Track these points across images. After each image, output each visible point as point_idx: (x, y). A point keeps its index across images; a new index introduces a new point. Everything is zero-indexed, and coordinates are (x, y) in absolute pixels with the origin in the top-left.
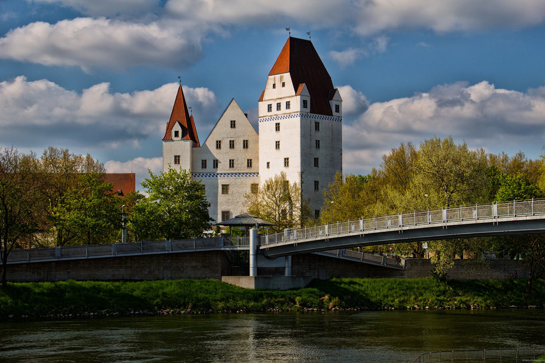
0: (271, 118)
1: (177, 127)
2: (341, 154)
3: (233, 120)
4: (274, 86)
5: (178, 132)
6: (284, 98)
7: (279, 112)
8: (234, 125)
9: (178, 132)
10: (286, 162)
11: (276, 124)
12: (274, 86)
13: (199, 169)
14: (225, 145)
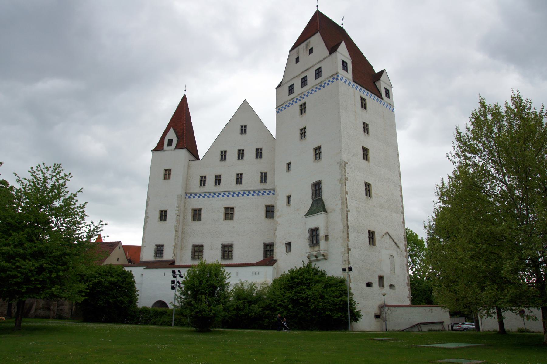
1: (172, 135)
2: (398, 155)
3: (243, 124)
5: (172, 140)
6: (311, 67)
8: (245, 130)
9: (172, 140)
10: (318, 151)
13: (195, 187)
14: (232, 156)
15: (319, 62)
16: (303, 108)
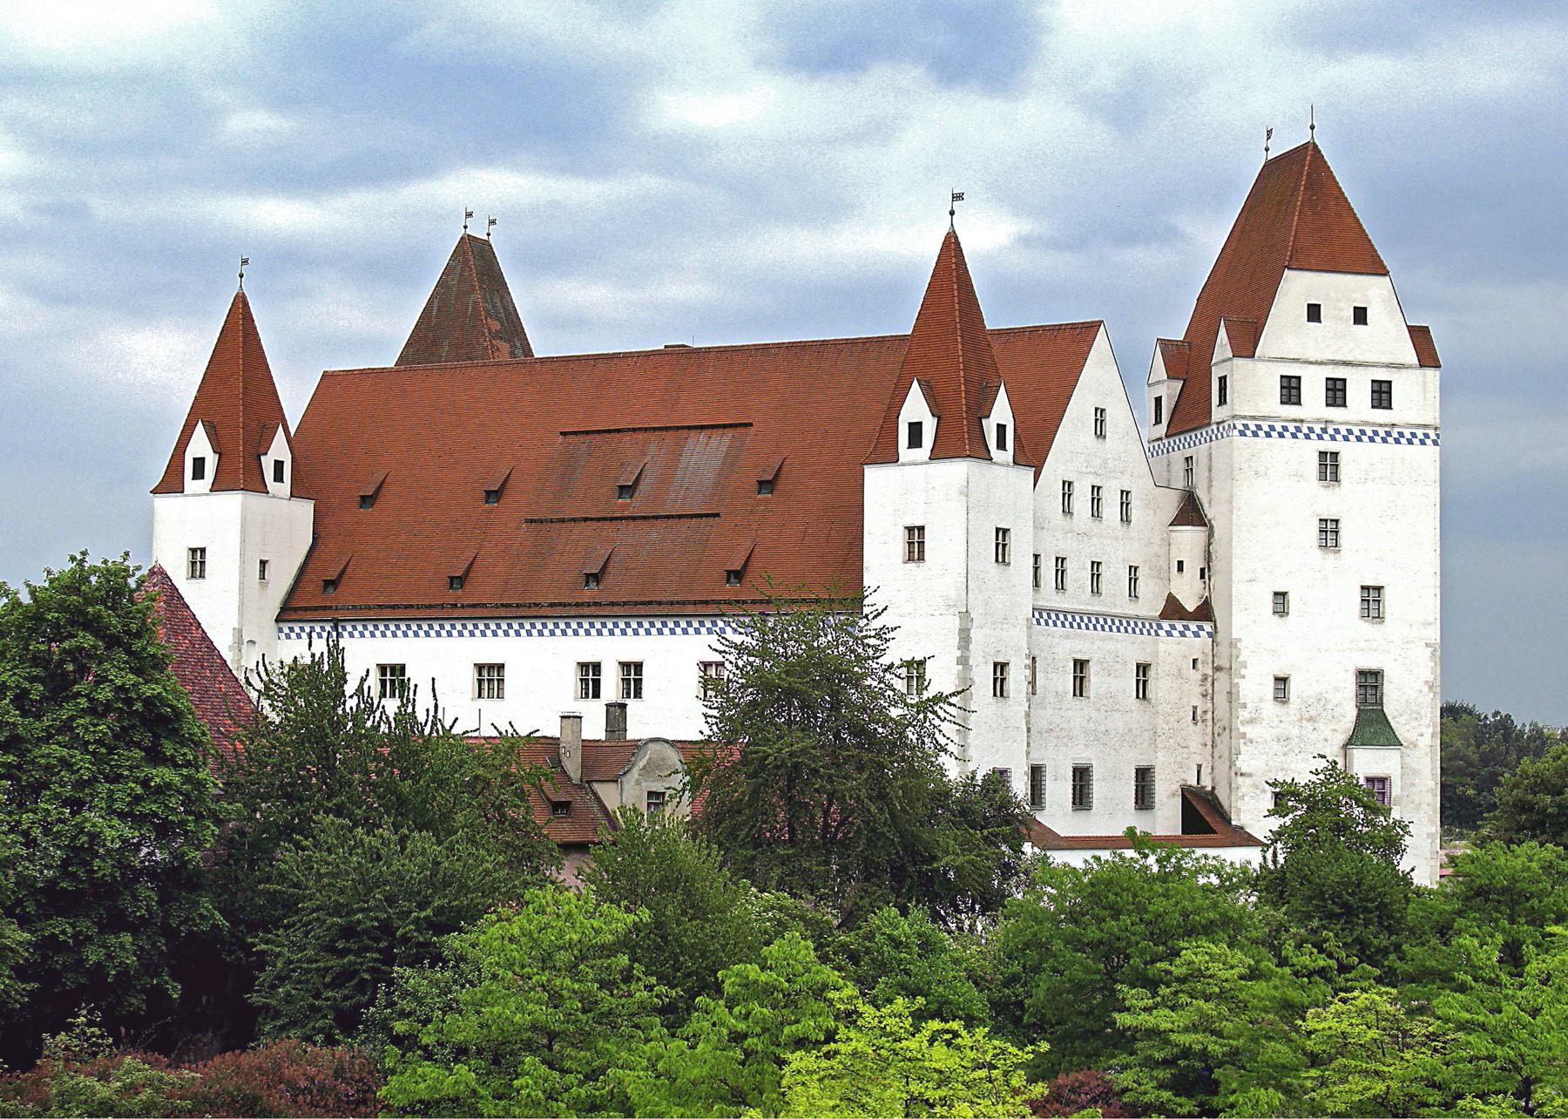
0: (1298, 430)
4: (1314, 313)
7: (1335, 413)
10: (1372, 597)
11: (1322, 454)
12: (1314, 313)
15: (1389, 366)
16: (1329, 466)
